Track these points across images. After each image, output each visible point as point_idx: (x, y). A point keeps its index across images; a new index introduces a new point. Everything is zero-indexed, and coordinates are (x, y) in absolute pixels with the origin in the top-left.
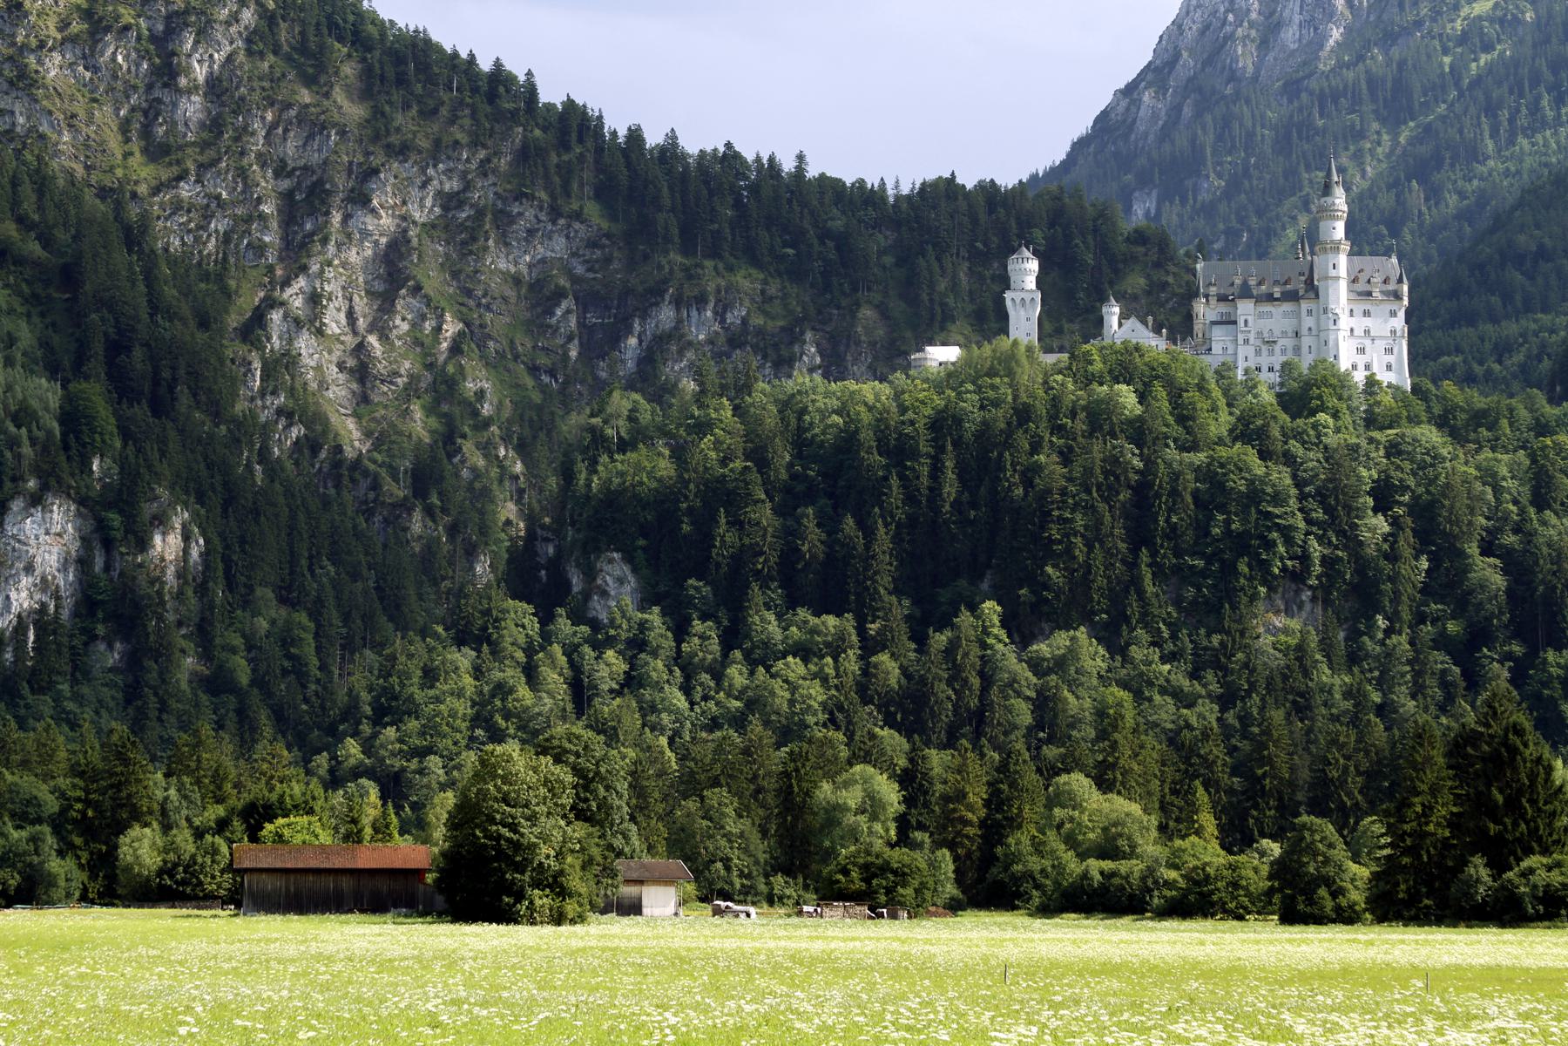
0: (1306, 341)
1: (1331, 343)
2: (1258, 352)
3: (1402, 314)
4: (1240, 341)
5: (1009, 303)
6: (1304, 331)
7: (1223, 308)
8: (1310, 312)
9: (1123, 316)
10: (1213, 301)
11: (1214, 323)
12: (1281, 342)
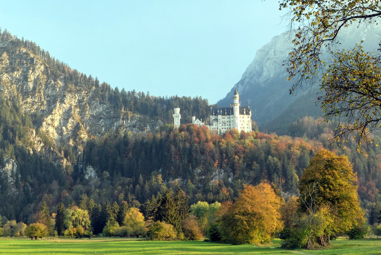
0: (231, 123)
1: (236, 124)
2: (222, 125)
3: (250, 117)
4: (219, 123)
5: (174, 117)
6: (231, 121)
7: (216, 117)
8: (232, 117)
9: (196, 119)
10: (214, 116)
11: (214, 120)
12: (227, 123)
